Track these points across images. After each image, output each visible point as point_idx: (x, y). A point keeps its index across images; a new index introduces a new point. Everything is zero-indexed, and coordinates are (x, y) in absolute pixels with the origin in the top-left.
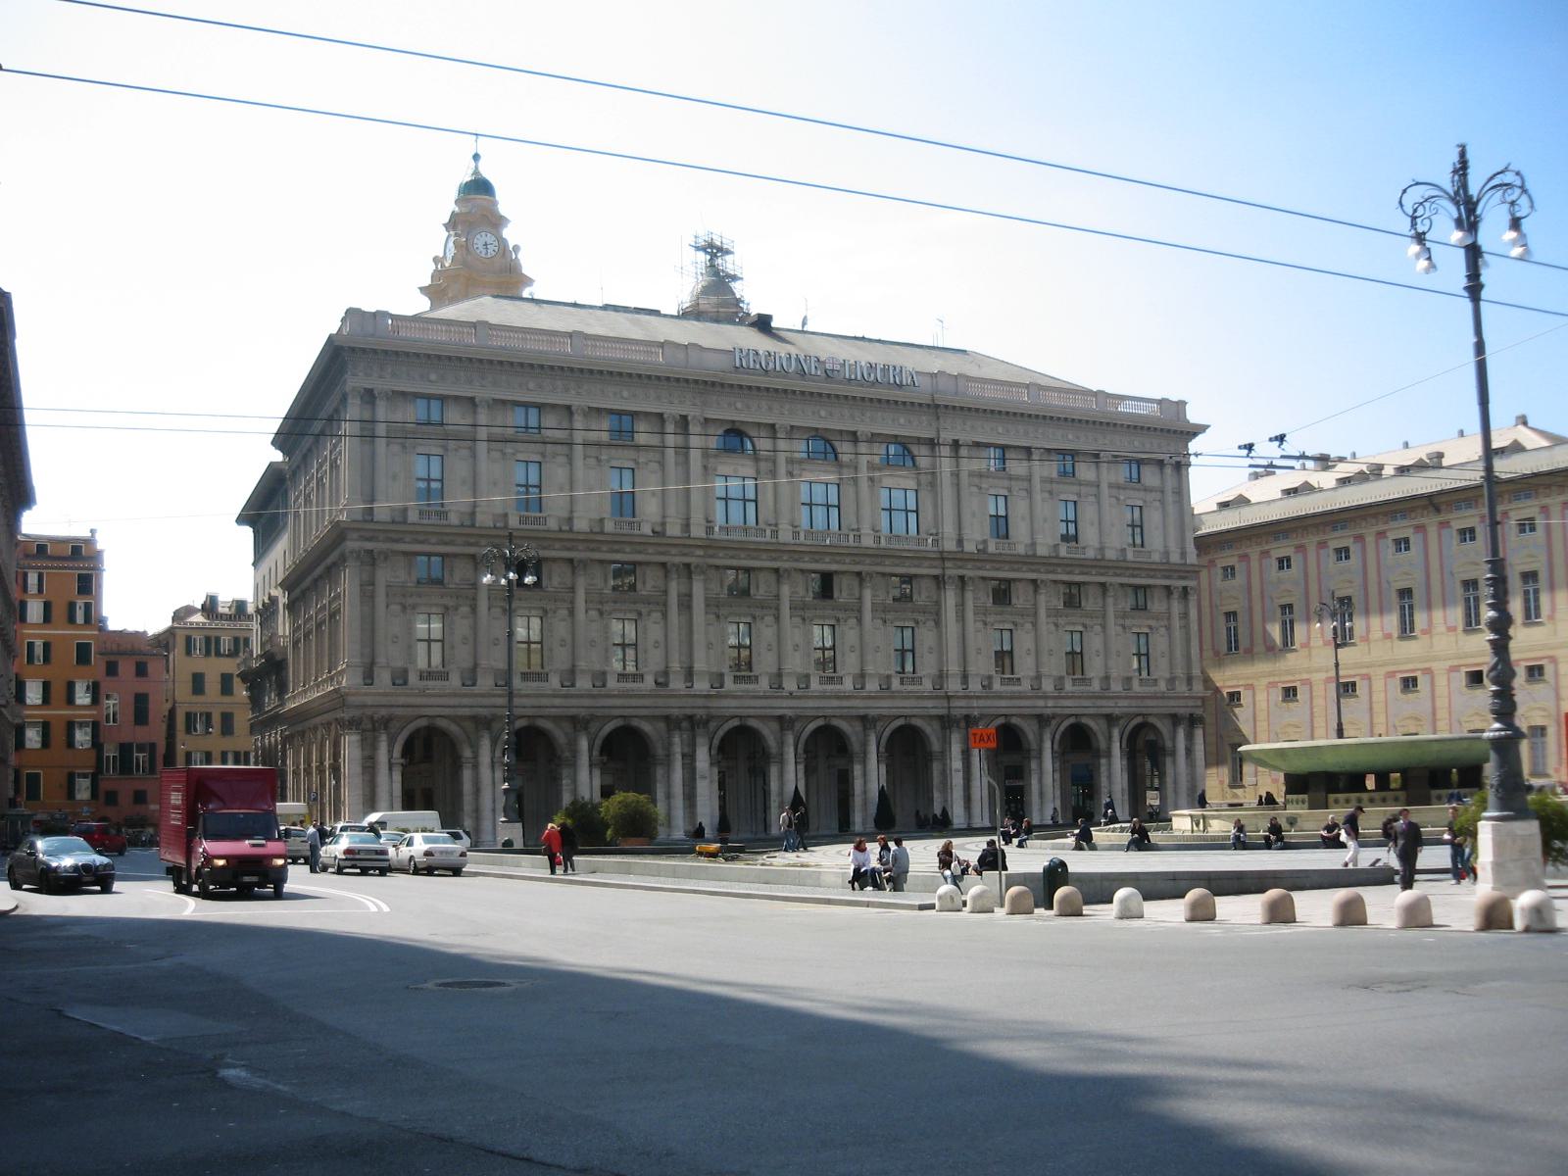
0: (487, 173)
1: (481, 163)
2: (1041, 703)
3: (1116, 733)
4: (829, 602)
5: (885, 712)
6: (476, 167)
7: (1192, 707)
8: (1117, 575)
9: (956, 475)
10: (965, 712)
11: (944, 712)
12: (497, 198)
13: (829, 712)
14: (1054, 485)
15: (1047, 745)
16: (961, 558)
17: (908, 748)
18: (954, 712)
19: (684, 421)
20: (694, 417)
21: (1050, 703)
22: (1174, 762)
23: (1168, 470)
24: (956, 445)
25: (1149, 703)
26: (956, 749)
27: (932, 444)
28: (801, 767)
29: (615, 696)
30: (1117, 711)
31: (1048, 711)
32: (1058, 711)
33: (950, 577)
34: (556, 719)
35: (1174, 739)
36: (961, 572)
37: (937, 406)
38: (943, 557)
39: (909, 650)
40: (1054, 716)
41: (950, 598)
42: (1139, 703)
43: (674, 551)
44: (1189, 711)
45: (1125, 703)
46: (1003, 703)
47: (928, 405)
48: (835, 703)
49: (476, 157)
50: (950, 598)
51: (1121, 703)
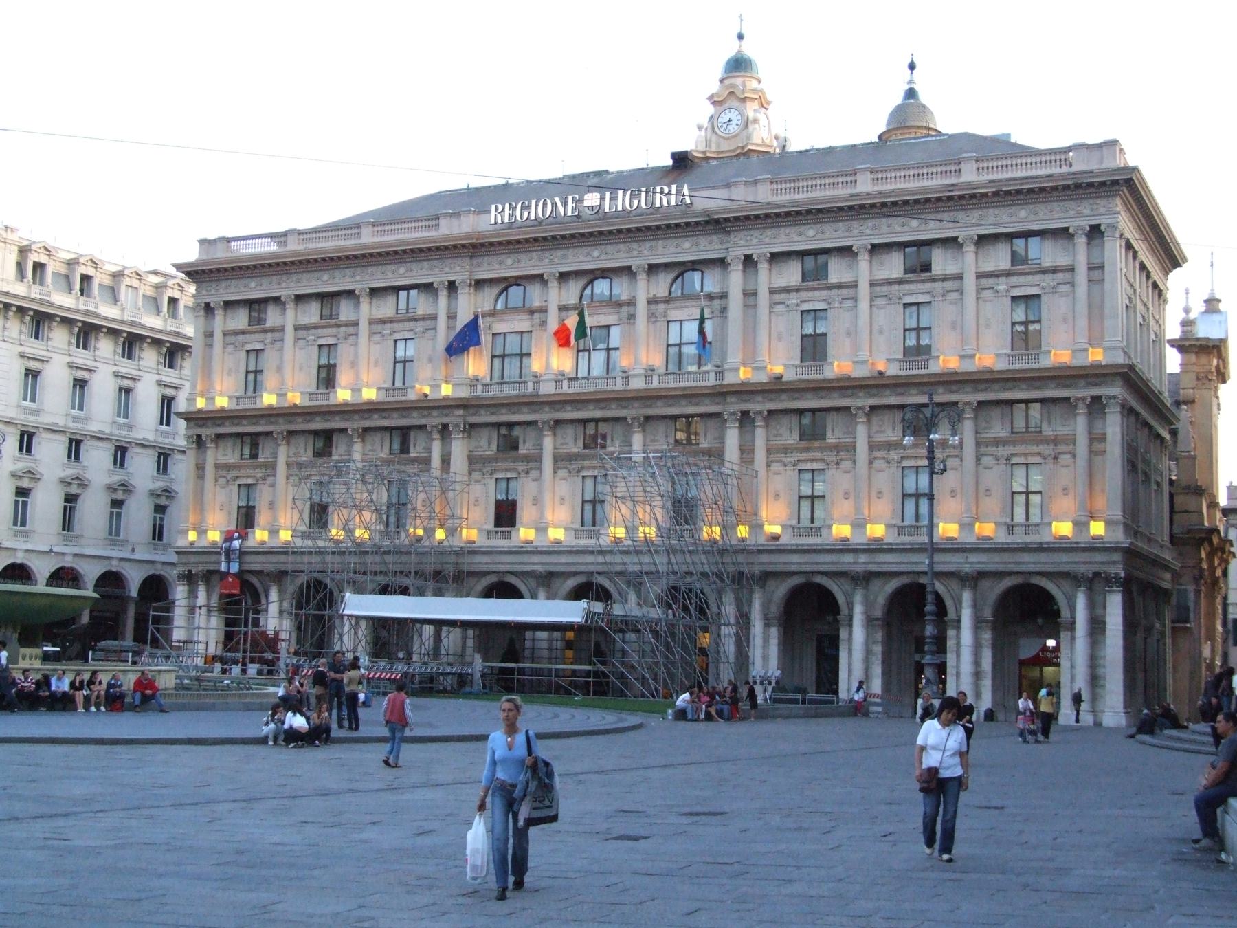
2: (848, 558)
4: (513, 453)
8: (977, 390)
9: (750, 294)
13: (591, 568)
14: (896, 287)
15: (858, 610)
16: (746, 391)
17: (913, 614)
19: (452, 287)
20: (463, 281)
21: (863, 558)
22: (1073, 638)
23: (1081, 241)
24: (749, 261)
25: (1027, 557)
26: (729, 610)
27: (721, 263)
28: (987, 636)
29: (541, 553)
30: (967, 568)
31: (859, 569)
33: (733, 414)
36: (744, 407)
37: (717, 221)
38: (721, 393)
39: (924, 495)
41: (732, 437)
42: (1006, 557)
43: (435, 413)
44: (1096, 568)
45: (983, 558)
46: (795, 558)
47: (707, 222)
50: (732, 437)
51: (973, 558)
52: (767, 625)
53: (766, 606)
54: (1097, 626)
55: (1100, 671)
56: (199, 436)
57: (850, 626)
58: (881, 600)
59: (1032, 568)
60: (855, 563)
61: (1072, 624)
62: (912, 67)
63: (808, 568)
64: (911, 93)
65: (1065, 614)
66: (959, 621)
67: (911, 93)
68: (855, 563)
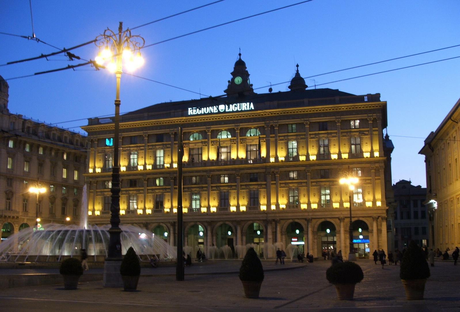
0: (243, 59)
1: (241, 57)
3: (342, 224)
5: (243, 219)
6: (240, 57)
7: (381, 213)
10: (273, 218)
11: (265, 218)
12: (247, 66)
15: (310, 229)
18: (270, 218)
22: (373, 235)
30: (342, 216)
31: (310, 217)
32: (314, 217)
34: (232, 222)
35: (372, 227)
40: (312, 219)
44: (379, 215)
48: (225, 216)
49: (240, 55)
52: (282, 235)
53: (281, 229)
54: (379, 231)
55: (380, 244)
56: (91, 182)
57: (308, 234)
58: (316, 226)
59: (361, 215)
60: (308, 215)
61: (372, 230)
62: (297, 66)
63: (294, 217)
64: (298, 74)
65: (370, 228)
66: (340, 231)
67: (298, 74)
68: (308, 215)
